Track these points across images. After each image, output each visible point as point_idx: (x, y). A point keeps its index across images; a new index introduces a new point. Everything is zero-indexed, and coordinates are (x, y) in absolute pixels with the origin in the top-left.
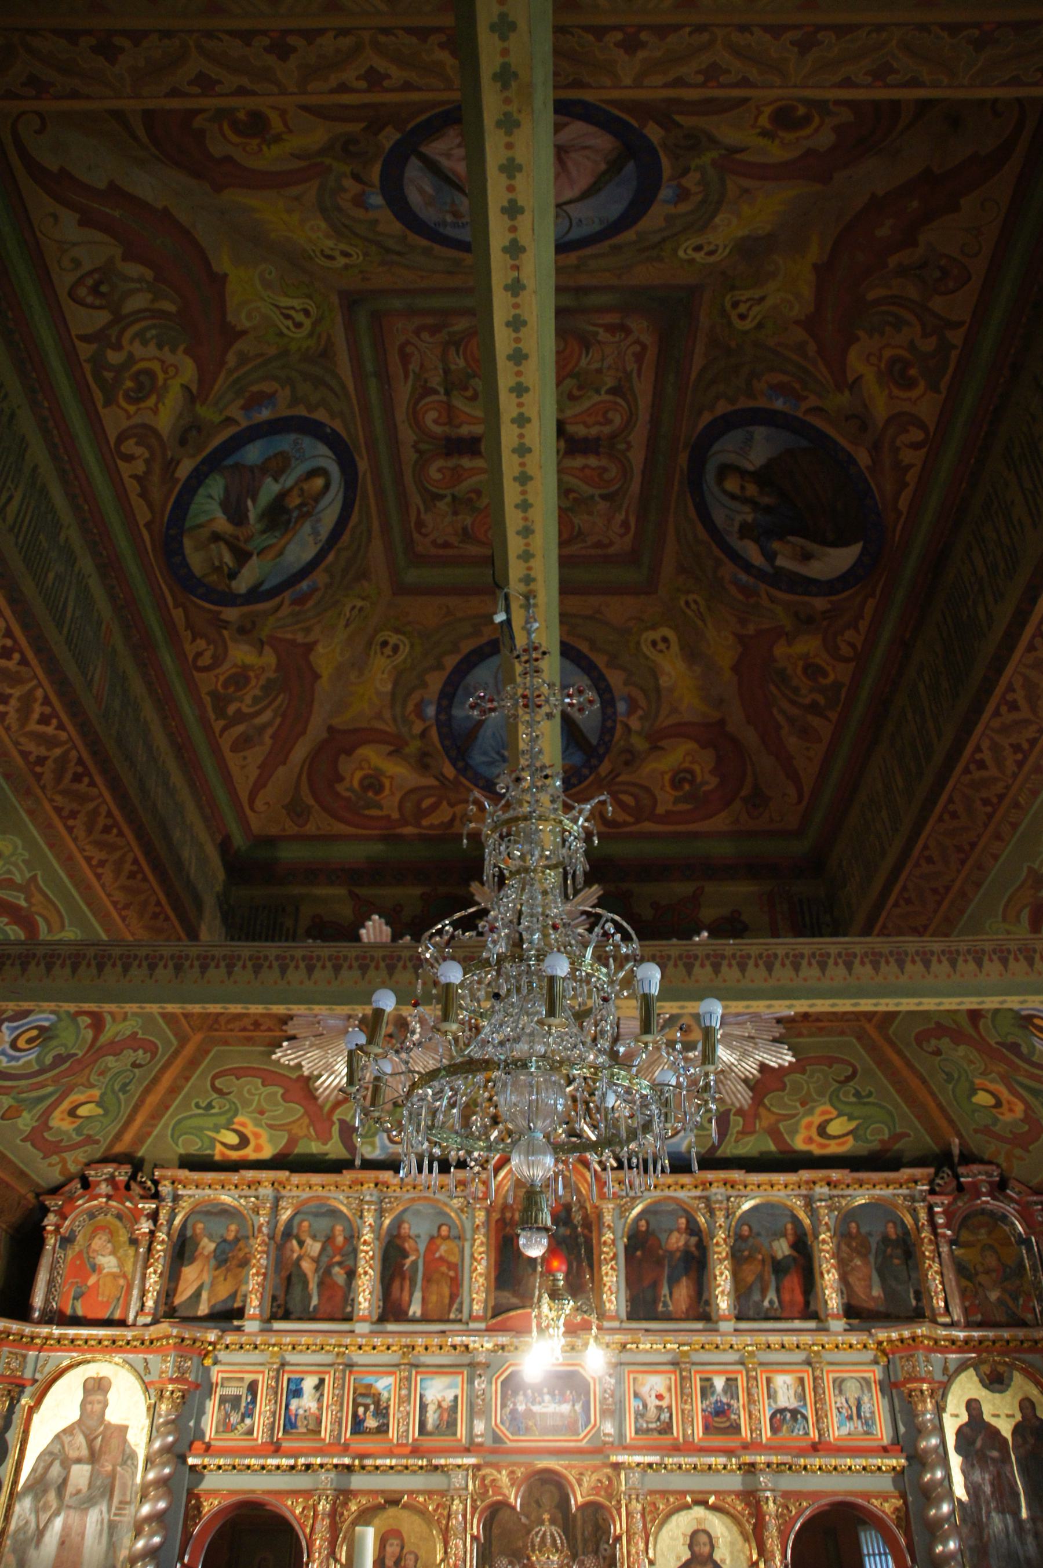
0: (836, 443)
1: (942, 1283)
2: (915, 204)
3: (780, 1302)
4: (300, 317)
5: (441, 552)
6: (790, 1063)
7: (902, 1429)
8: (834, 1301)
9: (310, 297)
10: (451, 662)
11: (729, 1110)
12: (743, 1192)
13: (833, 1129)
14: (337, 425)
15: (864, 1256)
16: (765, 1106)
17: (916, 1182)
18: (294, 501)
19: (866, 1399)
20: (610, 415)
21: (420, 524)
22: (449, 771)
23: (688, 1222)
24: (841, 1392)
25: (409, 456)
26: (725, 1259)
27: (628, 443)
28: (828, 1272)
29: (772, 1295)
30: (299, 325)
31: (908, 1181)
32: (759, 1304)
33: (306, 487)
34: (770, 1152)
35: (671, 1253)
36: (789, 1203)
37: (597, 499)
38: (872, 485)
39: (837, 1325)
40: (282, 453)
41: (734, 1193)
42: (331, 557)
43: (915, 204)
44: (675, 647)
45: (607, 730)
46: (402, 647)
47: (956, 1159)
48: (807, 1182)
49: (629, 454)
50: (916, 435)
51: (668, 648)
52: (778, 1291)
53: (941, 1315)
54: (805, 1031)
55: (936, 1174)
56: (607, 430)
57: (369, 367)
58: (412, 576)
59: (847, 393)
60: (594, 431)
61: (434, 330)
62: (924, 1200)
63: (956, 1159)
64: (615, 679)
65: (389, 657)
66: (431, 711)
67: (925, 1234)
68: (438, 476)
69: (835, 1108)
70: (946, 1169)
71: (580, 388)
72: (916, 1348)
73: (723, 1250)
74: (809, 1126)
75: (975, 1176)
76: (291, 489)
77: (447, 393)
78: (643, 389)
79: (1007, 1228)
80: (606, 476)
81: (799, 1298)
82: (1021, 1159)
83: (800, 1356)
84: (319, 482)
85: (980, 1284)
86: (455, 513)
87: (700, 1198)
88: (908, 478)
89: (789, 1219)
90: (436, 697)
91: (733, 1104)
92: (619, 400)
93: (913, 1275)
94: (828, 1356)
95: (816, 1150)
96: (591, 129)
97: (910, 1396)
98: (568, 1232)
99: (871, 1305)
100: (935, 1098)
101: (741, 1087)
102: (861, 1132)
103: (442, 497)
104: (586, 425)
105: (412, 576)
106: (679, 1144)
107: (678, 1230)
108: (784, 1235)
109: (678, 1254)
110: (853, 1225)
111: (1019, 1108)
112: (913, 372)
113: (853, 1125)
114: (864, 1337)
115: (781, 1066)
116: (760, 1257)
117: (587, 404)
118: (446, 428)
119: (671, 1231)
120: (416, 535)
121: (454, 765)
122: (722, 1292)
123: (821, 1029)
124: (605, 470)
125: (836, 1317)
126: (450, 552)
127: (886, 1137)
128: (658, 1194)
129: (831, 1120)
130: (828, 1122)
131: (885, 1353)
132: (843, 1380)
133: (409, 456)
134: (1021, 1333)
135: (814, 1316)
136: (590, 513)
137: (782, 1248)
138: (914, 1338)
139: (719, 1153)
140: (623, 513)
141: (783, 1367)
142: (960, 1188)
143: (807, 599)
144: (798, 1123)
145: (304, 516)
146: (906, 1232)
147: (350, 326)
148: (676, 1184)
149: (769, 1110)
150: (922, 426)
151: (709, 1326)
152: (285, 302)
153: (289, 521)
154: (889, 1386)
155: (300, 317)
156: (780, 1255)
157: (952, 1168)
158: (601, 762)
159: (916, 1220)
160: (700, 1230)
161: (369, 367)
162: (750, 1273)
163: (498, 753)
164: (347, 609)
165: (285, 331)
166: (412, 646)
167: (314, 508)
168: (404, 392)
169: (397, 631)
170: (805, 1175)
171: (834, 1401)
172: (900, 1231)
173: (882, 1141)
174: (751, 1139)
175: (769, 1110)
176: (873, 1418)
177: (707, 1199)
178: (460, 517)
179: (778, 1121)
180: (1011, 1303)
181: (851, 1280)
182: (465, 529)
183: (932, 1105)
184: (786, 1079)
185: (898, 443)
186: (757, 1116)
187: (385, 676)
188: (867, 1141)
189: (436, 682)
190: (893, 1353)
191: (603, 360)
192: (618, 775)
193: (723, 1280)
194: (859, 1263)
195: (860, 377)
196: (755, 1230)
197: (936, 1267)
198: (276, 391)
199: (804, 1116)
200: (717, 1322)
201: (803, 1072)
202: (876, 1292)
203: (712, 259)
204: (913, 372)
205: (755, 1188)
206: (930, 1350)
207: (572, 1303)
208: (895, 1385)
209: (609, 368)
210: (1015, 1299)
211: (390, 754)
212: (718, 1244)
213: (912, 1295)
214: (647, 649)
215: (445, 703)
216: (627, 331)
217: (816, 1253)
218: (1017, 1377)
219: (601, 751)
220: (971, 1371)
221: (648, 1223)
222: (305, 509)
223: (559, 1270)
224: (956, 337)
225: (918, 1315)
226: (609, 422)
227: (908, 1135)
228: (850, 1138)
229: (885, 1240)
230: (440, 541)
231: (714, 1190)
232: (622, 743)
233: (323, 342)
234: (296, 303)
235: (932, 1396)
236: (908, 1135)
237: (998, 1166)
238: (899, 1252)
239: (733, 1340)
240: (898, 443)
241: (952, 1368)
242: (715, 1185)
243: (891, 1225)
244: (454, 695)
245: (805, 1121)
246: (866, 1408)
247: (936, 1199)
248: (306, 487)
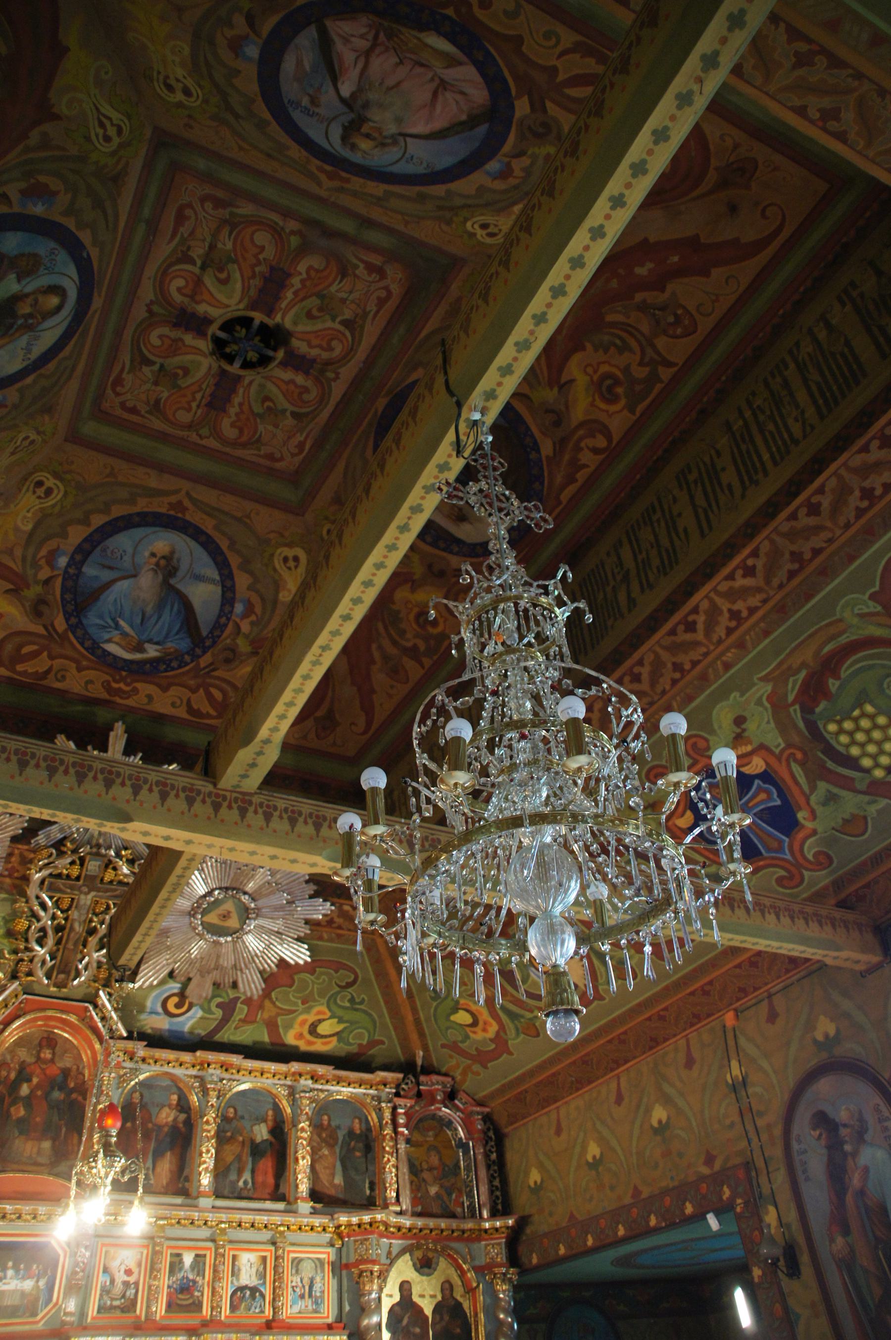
0: (528, 428)
1: (397, 1176)
2: (676, 259)
3: (253, 1183)
4: (112, 131)
5: (126, 415)
6: (306, 962)
7: (347, 1308)
8: (304, 1188)
9: (129, 117)
10: (98, 520)
11: (239, 998)
12: (236, 1076)
13: (323, 1029)
14: (94, 253)
15: (331, 1146)
16: (270, 999)
17: (385, 1085)
18: (25, 309)
19: (318, 1279)
20: (334, 343)
21: (119, 381)
22: (60, 624)
23: (179, 1099)
24: (297, 1271)
25: (139, 312)
26: (213, 1137)
27: (337, 374)
28: (303, 1158)
29: (247, 1176)
30: (107, 139)
31: (378, 1084)
32: (234, 1183)
33: (41, 298)
34: (263, 1043)
35: (160, 1127)
36: (274, 1091)
37: (288, 414)
38: (546, 474)
39: (305, 1207)
40: (36, 255)
41: (226, 1075)
42: (29, 380)
43: (676, 259)
44: (302, 569)
45: (218, 626)
46: (56, 492)
47: (419, 1069)
48: (294, 1074)
49: (333, 384)
50: (600, 442)
51: (296, 567)
52: (253, 1172)
53: (393, 1204)
54: (325, 936)
55: (404, 1079)
56: (325, 355)
57: (146, 212)
58: (89, 428)
59: (556, 390)
60: (314, 352)
61: (219, 204)
62: (390, 1101)
63: (419, 1069)
64: (242, 581)
65: (39, 497)
66: (63, 561)
67: (388, 1131)
68: (156, 342)
69: (330, 1010)
70: (411, 1076)
71: (320, 309)
72: (372, 1233)
73: (212, 1128)
74: (303, 1022)
75: (433, 1084)
76: (27, 295)
77: (203, 268)
78: (371, 332)
79: (449, 1133)
80: (305, 397)
81: (271, 1180)
82: (478, 1074)
83: (266, 1235)
84: (55, 301)
85: (424, 1180)
86: (156, 383)
87: (196, 1077)
88: (578, 476)
89: (271, 1106)
90: (71, 549)
91: (245, 993)
92: (348, 334)
93: (371, 1168)
94: (291, 1237)
95: (303, 1046)
96: (478, 78)
97: (360, 1275)
98: (62, 1096)
99: (332, 1192)
100: (414, 1010)
101: (257, 977)
102: (344, 1035)
103: (150, 363)
104: (310, 346)
105: (89, 428)
106: (184, 1024)
107: (170, 1106)
108: (265, 1121)
109: (166, 1129)
110: (326, 1117)
111: (494, 1028)
112: (619, 390)
113: (340, 1027)
114: (325, 1220)
115: (297, 964)
116: (241, 1139)
117: (319, 326)
118: (186, 300)
119: (163, 1106)
120: (109, 391)
121: (67, 620)
122: (206, 1169)
123: (339, 936)
124: (306, 390)
125: (303, 1199)
126: (134, 418)
127: (365, 1042)
128: (157, 1069)
129: (324, 1020)
130: (320, 1021)
131: (340, 1236)
132: (301, 1260)
133: (139, 312)
134: (454, 1224)
135: (281, 1198)
136: (276, 426)
137: (262, 1133)
138: (371, 1224)
139: (218, 1038)
140: (304, 435)
141: (248, 1245)
142: (419, 1095)
143: (444, 554)
144: (294, 1019)
145: (30, 328)
146: (369, 1129)
147: (148, 166)
148: (177, 1060)
149: (274, 1003)
150: (609, 436)
151: (189, 1201)
152: (107, 110)
153: (11, 326)
154: (340, 1267)
155: (112, 131)
156: (258, 1139)
157: (416, 1077)
158: (204, 653)
159: (381, 1118)
160: (190, 1108)
161: (146, 212)
162: (231, 1152)
163: (113, 620)
164: (21, 436)
165: (94, 138)
166: (66, 494)
167: (39, 323)
168: (164, 249)
169: (56, 475)
170: (295, 1066)
171: (292, 1280)
172: (364, 1125)
173: (360, 1045)
174: (249, 1028)
175: (274, 1003)
176: (322, 1297)
177: (201, 1079)
178: (159, 388)
179: (278, 1015)
180: (445, 1198)
181: (318, 1167)
182: (157, 402)
183: (410, 1018)
184: (296, 977)
185: (583, 445)
186: (261, 1007)
187: (30, 515)
188: (350, 1044)
189: (77, 535)
190: (349, 1237)
191: (351, 292)
192: (214, 670)
193: (208, 1159)
194: (326, 1152)
195: (572, 381)
196: (240, 1113)
197: (393, 1160)
198: (58, 192)
199: (301, 1014)
200: (197, 1198)
201: (312, 974)
202: (338, 1180)
203: (489, 241)
204: (619, 390)
205: (247, 1073)
206: (382, 1236)
207: (123, 1161)
208: (347, 1266)
209: (353, 302)
210: (449, 1195)
211: (7, 592)
212: (207, 1122)
213: (367, 1185)
214: (278, 563)
215: (78, 557)
216: (381, 272)
217: (292, 1141)
218: (443, 1263)
219: (208, 643)
220: (407, 1256)
221: (142, 1095)
222: (30, 321)
223: (113, 1126)
224: (665, 374)
225: (369, 1204)
226: (330, 349)
227: (382, 1043)
228: (335, 1039)
229: (351, 1133)
230: (129, 404)
231: (211, 1071)
232: (228, 641)
233: (120, 167)
234: (115, 115)
235: (379, 1277)
236: (382, 1043)
237: (453, 1079)
238: (361, 1145)
239: (210, 1216)
240: (583, 445)
241: (395, 1252)
242: (213, 1066)
243: (357, 1121)
244: (89, 553)
245: (302, 1017)
246: (317, 1287)
247: (398, 1101)
248: (41, 298)
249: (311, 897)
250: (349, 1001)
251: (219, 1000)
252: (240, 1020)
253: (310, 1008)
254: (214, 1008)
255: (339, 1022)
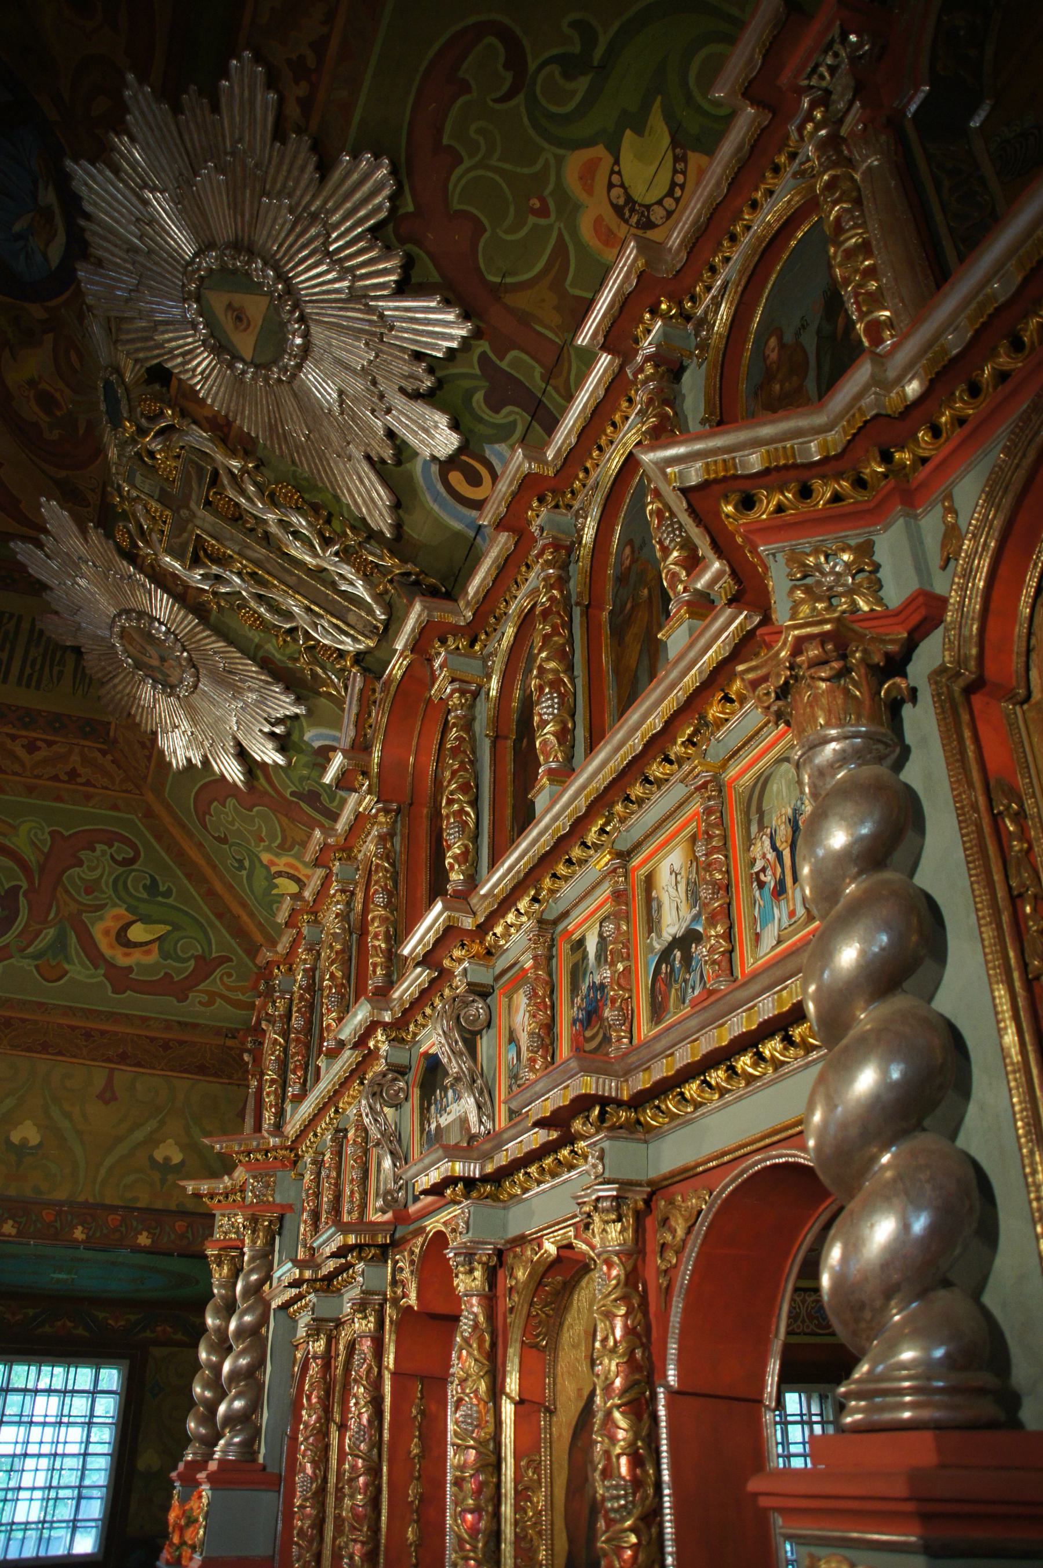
144: (582, 248)
179: (558, 286)
249: (215, 109)
250: (568, 76)
251: (479, 397)
252: (547, 378)
253: (564, 199)
254: (500, 418)
255: (639, 130)
